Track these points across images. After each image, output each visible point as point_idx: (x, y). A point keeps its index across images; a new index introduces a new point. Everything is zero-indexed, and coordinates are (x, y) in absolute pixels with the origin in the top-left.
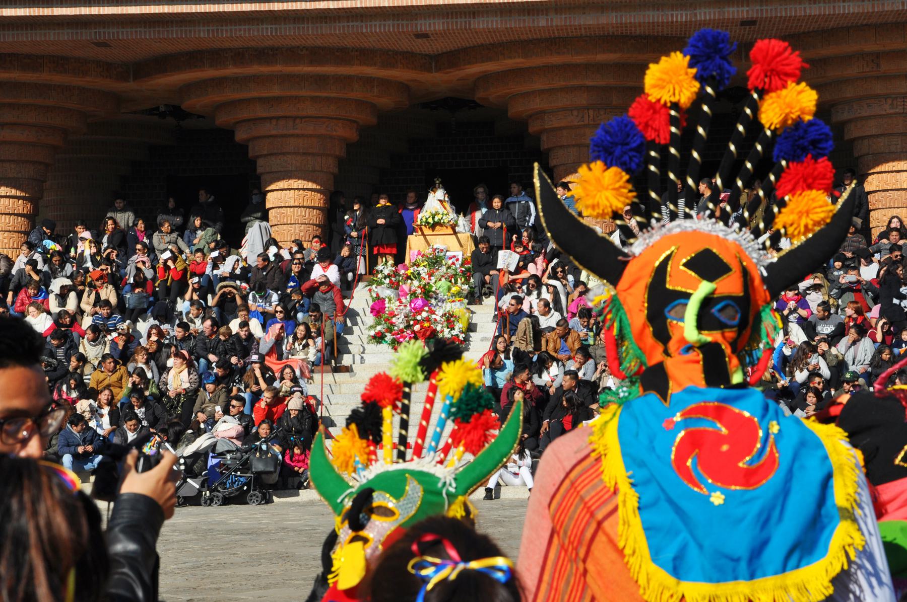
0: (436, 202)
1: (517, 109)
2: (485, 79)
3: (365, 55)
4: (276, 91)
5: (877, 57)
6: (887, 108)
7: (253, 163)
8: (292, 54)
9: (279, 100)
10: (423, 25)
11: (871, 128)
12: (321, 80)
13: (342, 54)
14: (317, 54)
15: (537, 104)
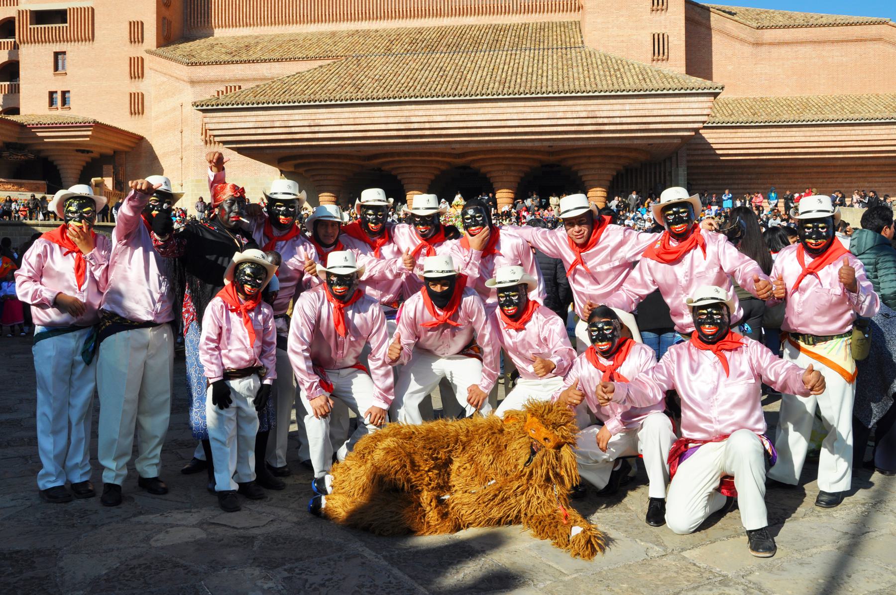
0: (458, 199)
1: (483, 170)
2: (474, 161)
3: (437, 154)
4: (410, 165)
5: (590, 157)
6: (593, 172)
7: (402, 186)
8: (414, 154)
9: (411, 167)
10: (453, 146)
11: (589, 178)
12: (423, 161)
13: (430, 154)
14: (422, 154)
15: (489, 169)
